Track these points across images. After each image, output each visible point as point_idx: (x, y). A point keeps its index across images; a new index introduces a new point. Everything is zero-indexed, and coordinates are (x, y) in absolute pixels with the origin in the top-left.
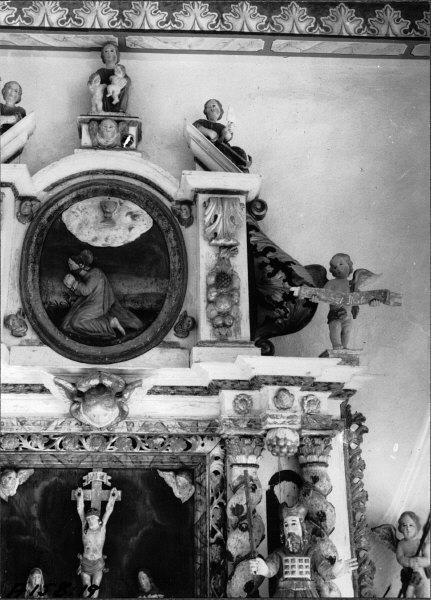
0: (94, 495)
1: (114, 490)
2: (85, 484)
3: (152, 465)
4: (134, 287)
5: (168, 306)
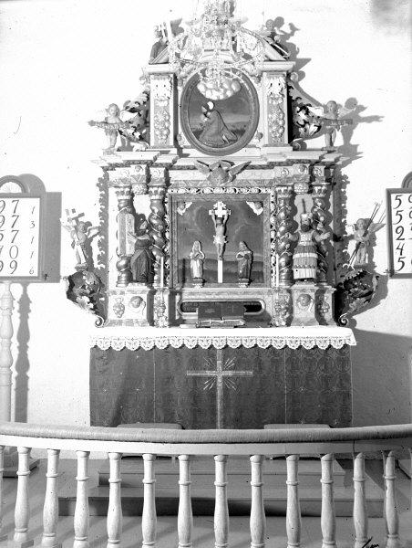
4: (231, 120)
5: (251, 127)
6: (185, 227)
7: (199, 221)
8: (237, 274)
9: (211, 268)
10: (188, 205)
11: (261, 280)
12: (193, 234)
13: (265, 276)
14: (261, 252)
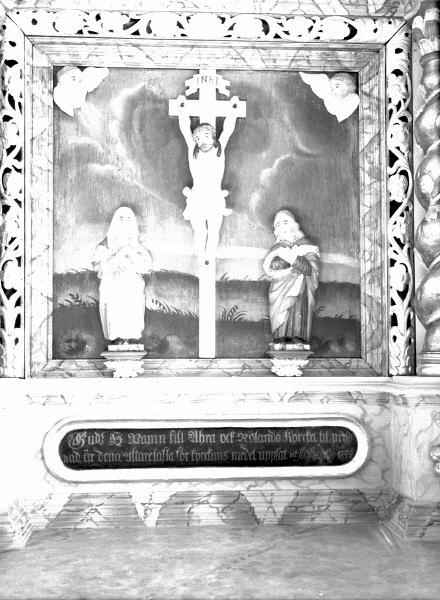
0: (208, 109)
1: (235, 99)
2: (188, 93)
3: (294, 65)
6: (85, 155)
7: (137, 135)
8: (266, 324)
9: (175, 301)
10: (92, 79)
11: (350, 347)
12: (110, 182)
13: (366, 333)
14: (354, 250)
